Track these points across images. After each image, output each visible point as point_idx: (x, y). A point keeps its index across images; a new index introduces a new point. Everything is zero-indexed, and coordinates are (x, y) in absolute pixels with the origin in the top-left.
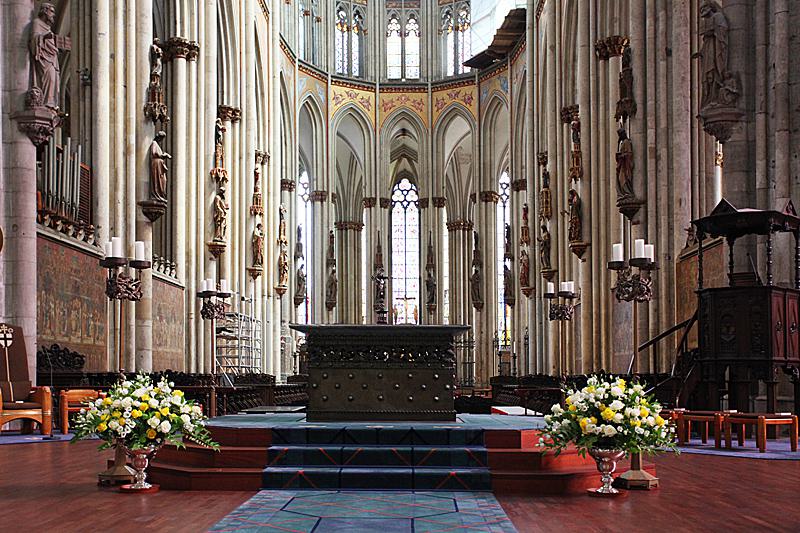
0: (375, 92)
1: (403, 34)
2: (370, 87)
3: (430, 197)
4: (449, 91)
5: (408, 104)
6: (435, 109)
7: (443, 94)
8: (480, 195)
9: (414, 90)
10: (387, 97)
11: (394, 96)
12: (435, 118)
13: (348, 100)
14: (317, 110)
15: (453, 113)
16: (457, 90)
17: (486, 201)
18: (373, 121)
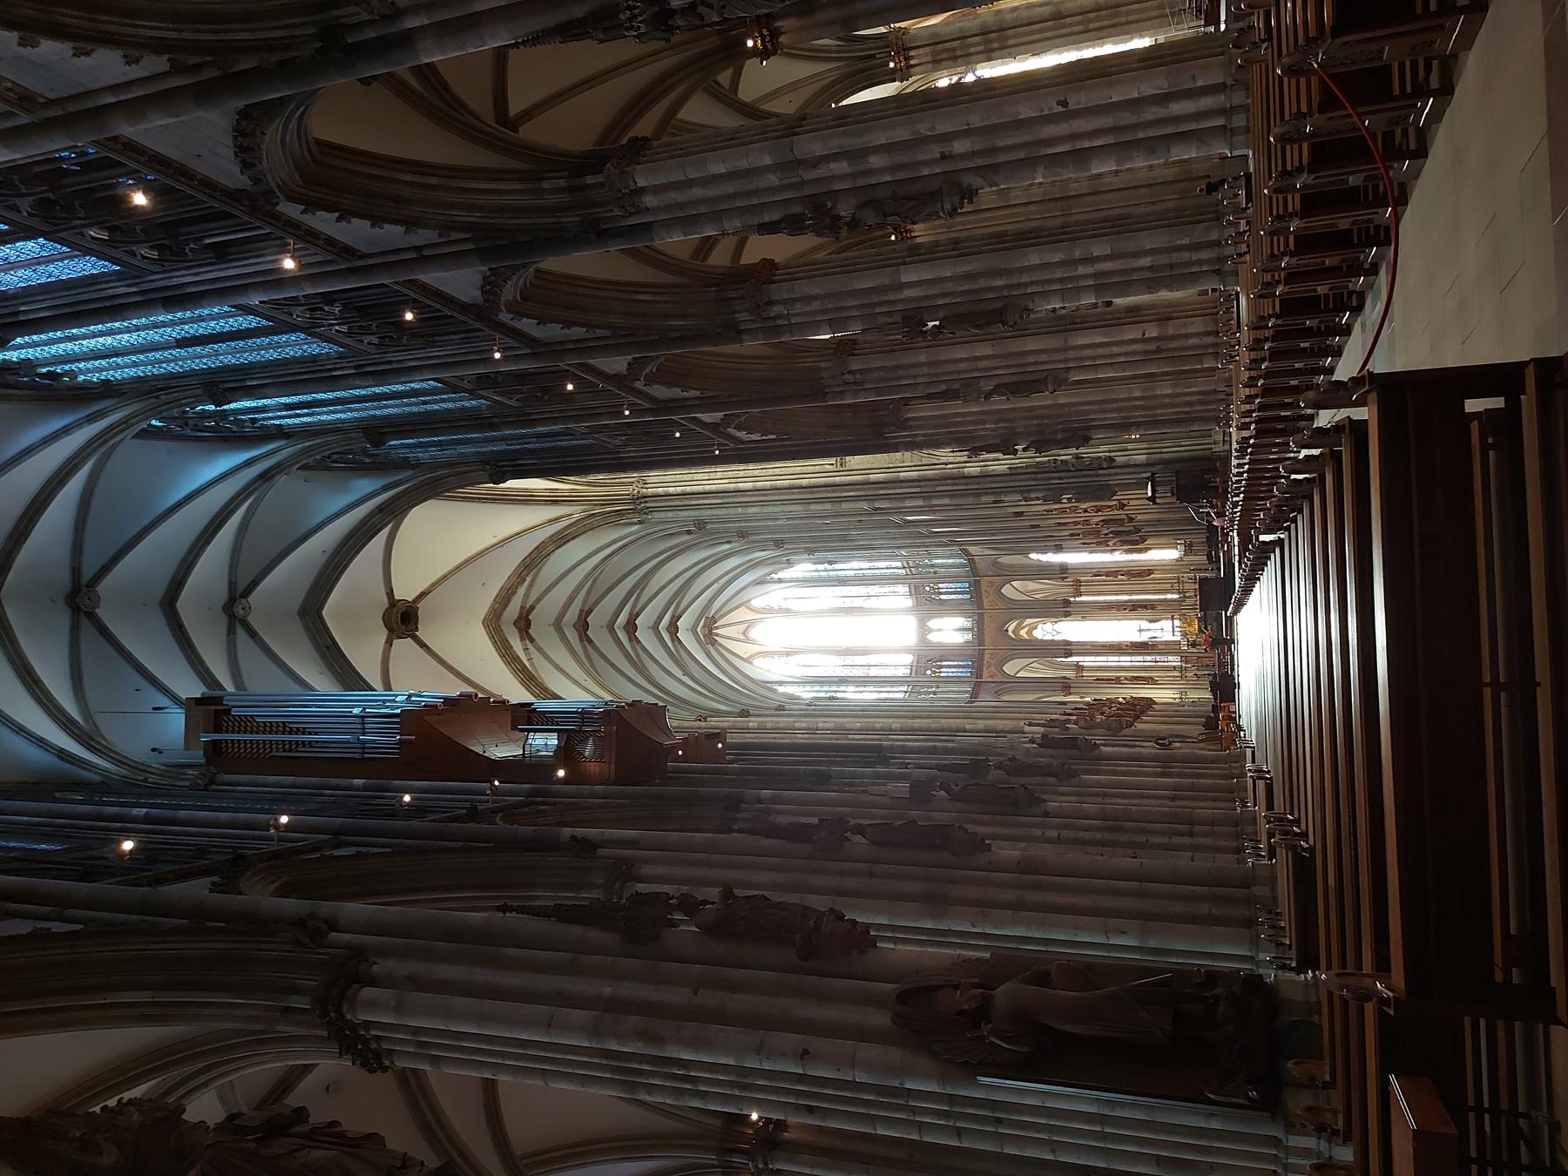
2: (981, 653)
11: (987, 636)
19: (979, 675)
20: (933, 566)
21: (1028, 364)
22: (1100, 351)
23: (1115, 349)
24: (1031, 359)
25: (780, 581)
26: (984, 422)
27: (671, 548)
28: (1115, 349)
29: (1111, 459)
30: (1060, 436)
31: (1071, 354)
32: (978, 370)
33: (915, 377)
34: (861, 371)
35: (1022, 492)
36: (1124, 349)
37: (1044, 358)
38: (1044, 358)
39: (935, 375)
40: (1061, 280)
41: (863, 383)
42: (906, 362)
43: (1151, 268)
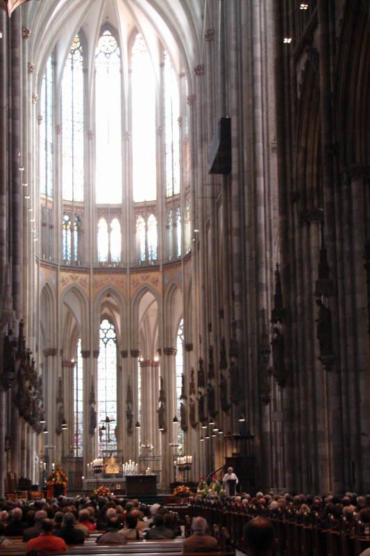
0: (90, 274)
1: (110, 230)
2: (86, 271)
3: (129, 350)
4: (142, 274)
5: (113, 283)
6: (132, 286)
7: (138, 277)
8: (164, 351)
9: (117, 273)
10: (98, 277)
12: (132, 292)
13: (71, 282)
14: (51, 292)
15: (145, 289)
16: (148, 274)
17: (168, 354)
18: (88, 293)
19: (65, 268)
20: (175, 225)
21: (345, 338)
23: (353, 411)
24: (350, 341)
25: (162, 65)
26: (302, 294)
28: (353, 411)
29: (267, 401)
30: (286, 361)
33: (342, 240)
34: (349, 190)
35: (241, 321)
36: (353, 416)
37: (350, 352)
39: (342, 258)
41: (340, 191)
42: (356, 232)
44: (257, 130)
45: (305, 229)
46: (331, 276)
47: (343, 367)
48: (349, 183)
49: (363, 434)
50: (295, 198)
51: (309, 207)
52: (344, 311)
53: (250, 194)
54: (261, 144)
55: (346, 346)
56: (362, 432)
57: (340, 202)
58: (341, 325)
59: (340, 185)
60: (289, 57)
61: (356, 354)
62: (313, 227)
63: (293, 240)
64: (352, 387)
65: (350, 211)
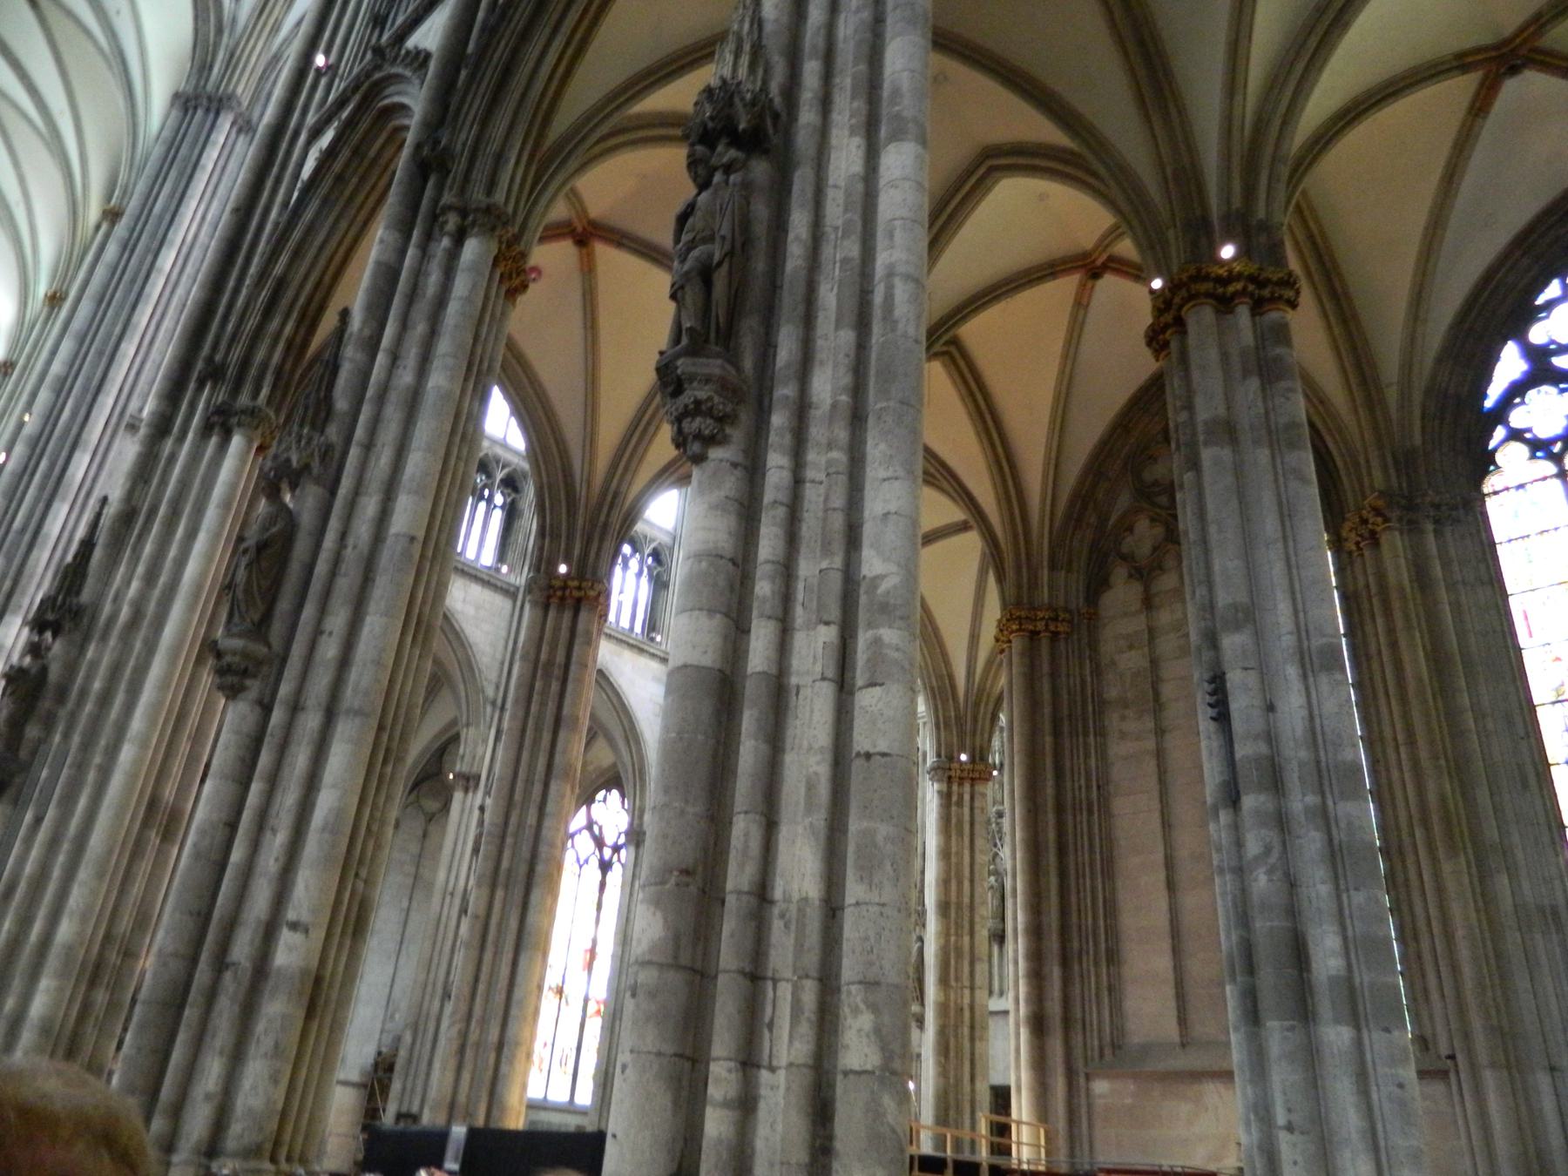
22: (288, 798)
23: (276, 842)
24: (337, 621)
26: (150, 578)
27: (85, 186)
30: (32, 731)
31: (310, 722)
32: (357, 492)
33: (395, 357)
34: (453, 255)
37: (329, 650)
38: (329, 650)
40: (787, 571)
41: (424, 249)
42: (444, 346)
43: (762, 893)
44: (111, 374)
45: (214, 440)
46: (333, 432)
47: (285, 689)
48: (459, 239)
49: (294, 926)
50: (214, 373)
51: (244, 399)
52: (343, 536)
53: (47, 477)
54: (110, 401)
55: (318, 632)
56: (291, 915)
57: (418, 274)
58: (321, 568)
59: (428, 237)
60: (296, 134)
61: (344, 662)
62: (237, 441)
63: (172, 458)
64: (300, 759)
65: (441, 302)
